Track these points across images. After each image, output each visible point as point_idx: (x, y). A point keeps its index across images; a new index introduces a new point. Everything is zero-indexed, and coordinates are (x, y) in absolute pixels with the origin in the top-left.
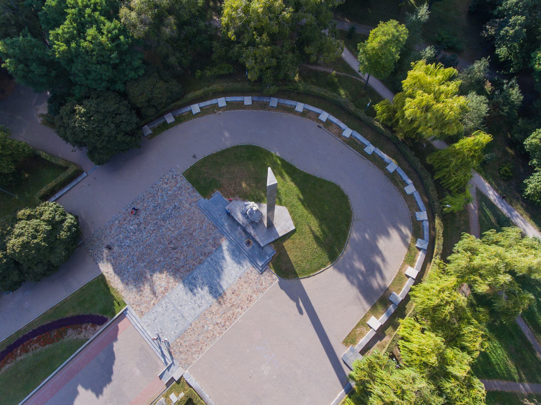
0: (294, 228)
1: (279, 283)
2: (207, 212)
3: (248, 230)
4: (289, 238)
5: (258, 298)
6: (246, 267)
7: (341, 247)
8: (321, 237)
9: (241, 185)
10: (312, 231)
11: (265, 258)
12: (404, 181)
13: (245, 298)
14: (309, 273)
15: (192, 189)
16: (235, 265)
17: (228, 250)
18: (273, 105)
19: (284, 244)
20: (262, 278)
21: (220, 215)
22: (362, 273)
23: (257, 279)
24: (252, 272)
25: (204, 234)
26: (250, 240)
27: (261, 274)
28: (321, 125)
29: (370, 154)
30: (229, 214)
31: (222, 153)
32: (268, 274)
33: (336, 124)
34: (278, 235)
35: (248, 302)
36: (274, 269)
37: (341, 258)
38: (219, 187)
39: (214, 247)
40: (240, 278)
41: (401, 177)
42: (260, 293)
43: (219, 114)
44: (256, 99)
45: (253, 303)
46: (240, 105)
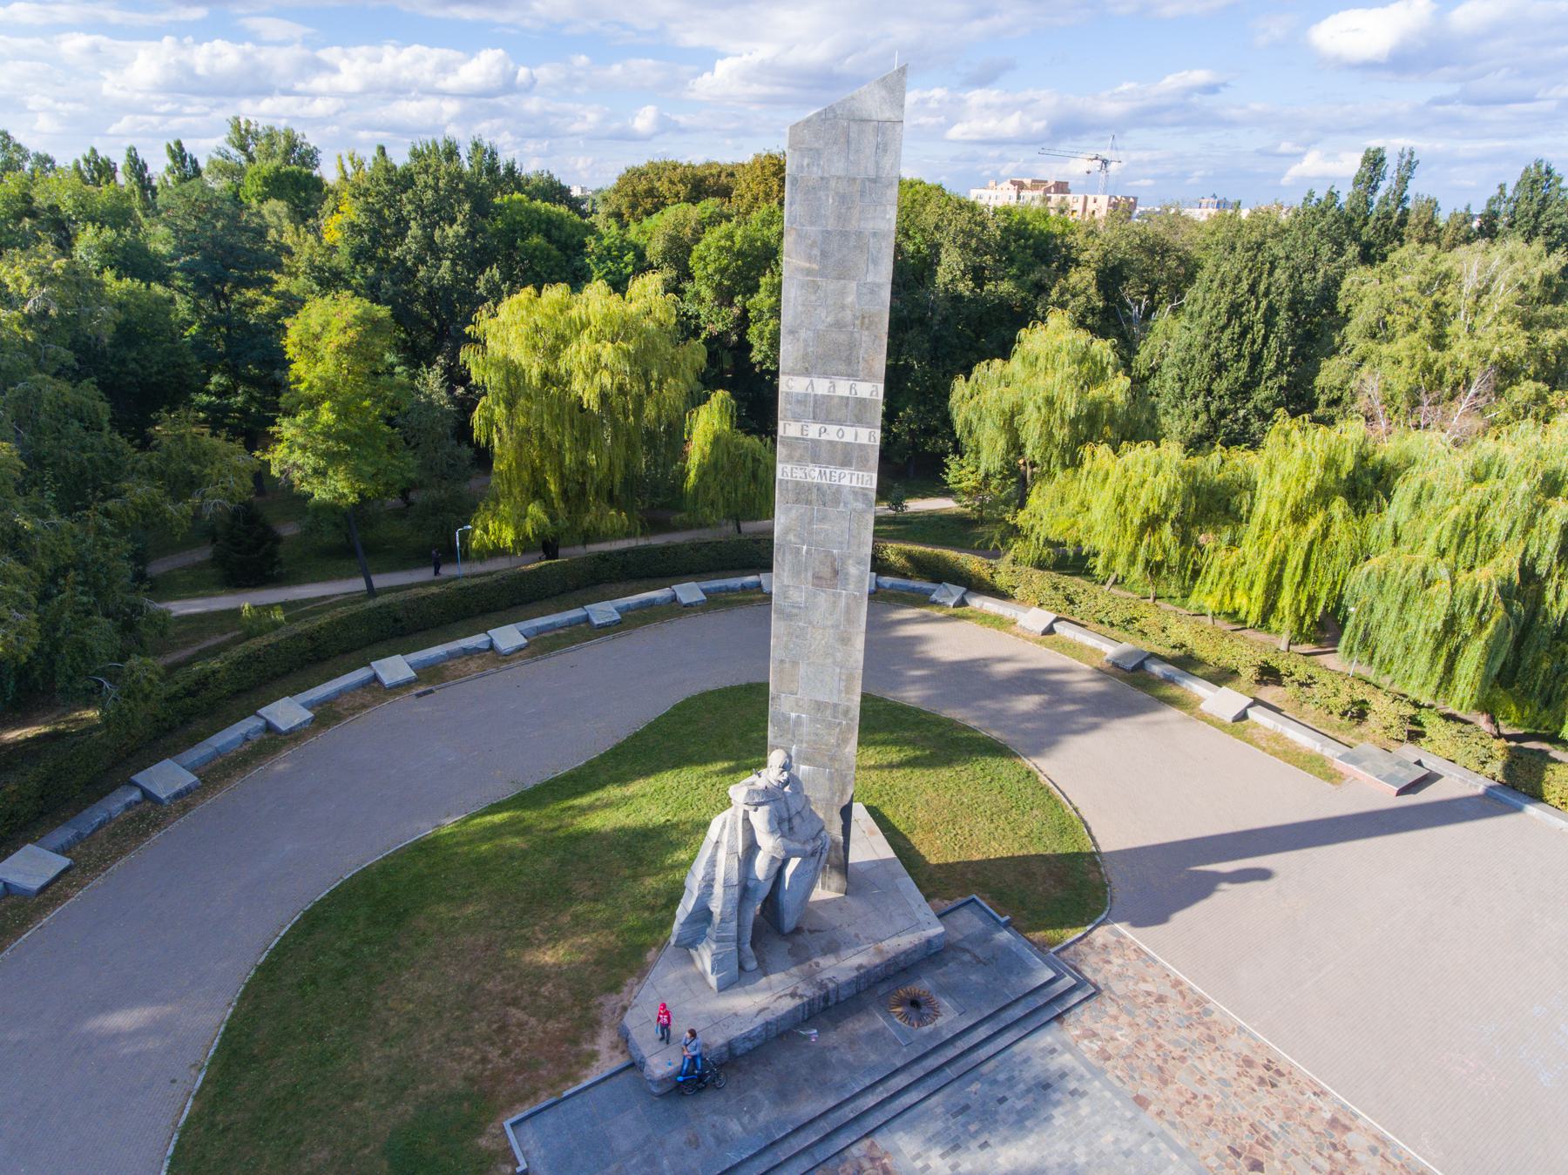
1: (1137, 923)
3: (842, 978)
4: (904, 837)
5: (1241, 1029)
6: (1066, 1060)
7: (952, 724)
8: (909, 753)
9: (542, 974)
10: (880, 767)
11: (1005, 950)
12: (744, 587)
13: (1267, 1098)
14: (1063, 815)
16: (1059, 1117)
17: (956, 1147)
18: (179, 786)
19: (933, 860)
20: (1119, 987)
21: (695, 1143)
22: (1050, 704)
23: (1129, 1013)
24: (1095, 1035)
26: (895, 983)
27: (1098, 992)
28: (422, 689)
29: (618, 617)
30: (701, 1077)
32: (1093, 959)
33: (452, 656)
34: (884, 863)
35: (1283, 1084)
36: (1062, 925)
37: (995, 734)
38: (482, 1102)
40: (1141, 1101)
42: (1208, 1012)
44: (63, 835)
45: (1286, 1058)
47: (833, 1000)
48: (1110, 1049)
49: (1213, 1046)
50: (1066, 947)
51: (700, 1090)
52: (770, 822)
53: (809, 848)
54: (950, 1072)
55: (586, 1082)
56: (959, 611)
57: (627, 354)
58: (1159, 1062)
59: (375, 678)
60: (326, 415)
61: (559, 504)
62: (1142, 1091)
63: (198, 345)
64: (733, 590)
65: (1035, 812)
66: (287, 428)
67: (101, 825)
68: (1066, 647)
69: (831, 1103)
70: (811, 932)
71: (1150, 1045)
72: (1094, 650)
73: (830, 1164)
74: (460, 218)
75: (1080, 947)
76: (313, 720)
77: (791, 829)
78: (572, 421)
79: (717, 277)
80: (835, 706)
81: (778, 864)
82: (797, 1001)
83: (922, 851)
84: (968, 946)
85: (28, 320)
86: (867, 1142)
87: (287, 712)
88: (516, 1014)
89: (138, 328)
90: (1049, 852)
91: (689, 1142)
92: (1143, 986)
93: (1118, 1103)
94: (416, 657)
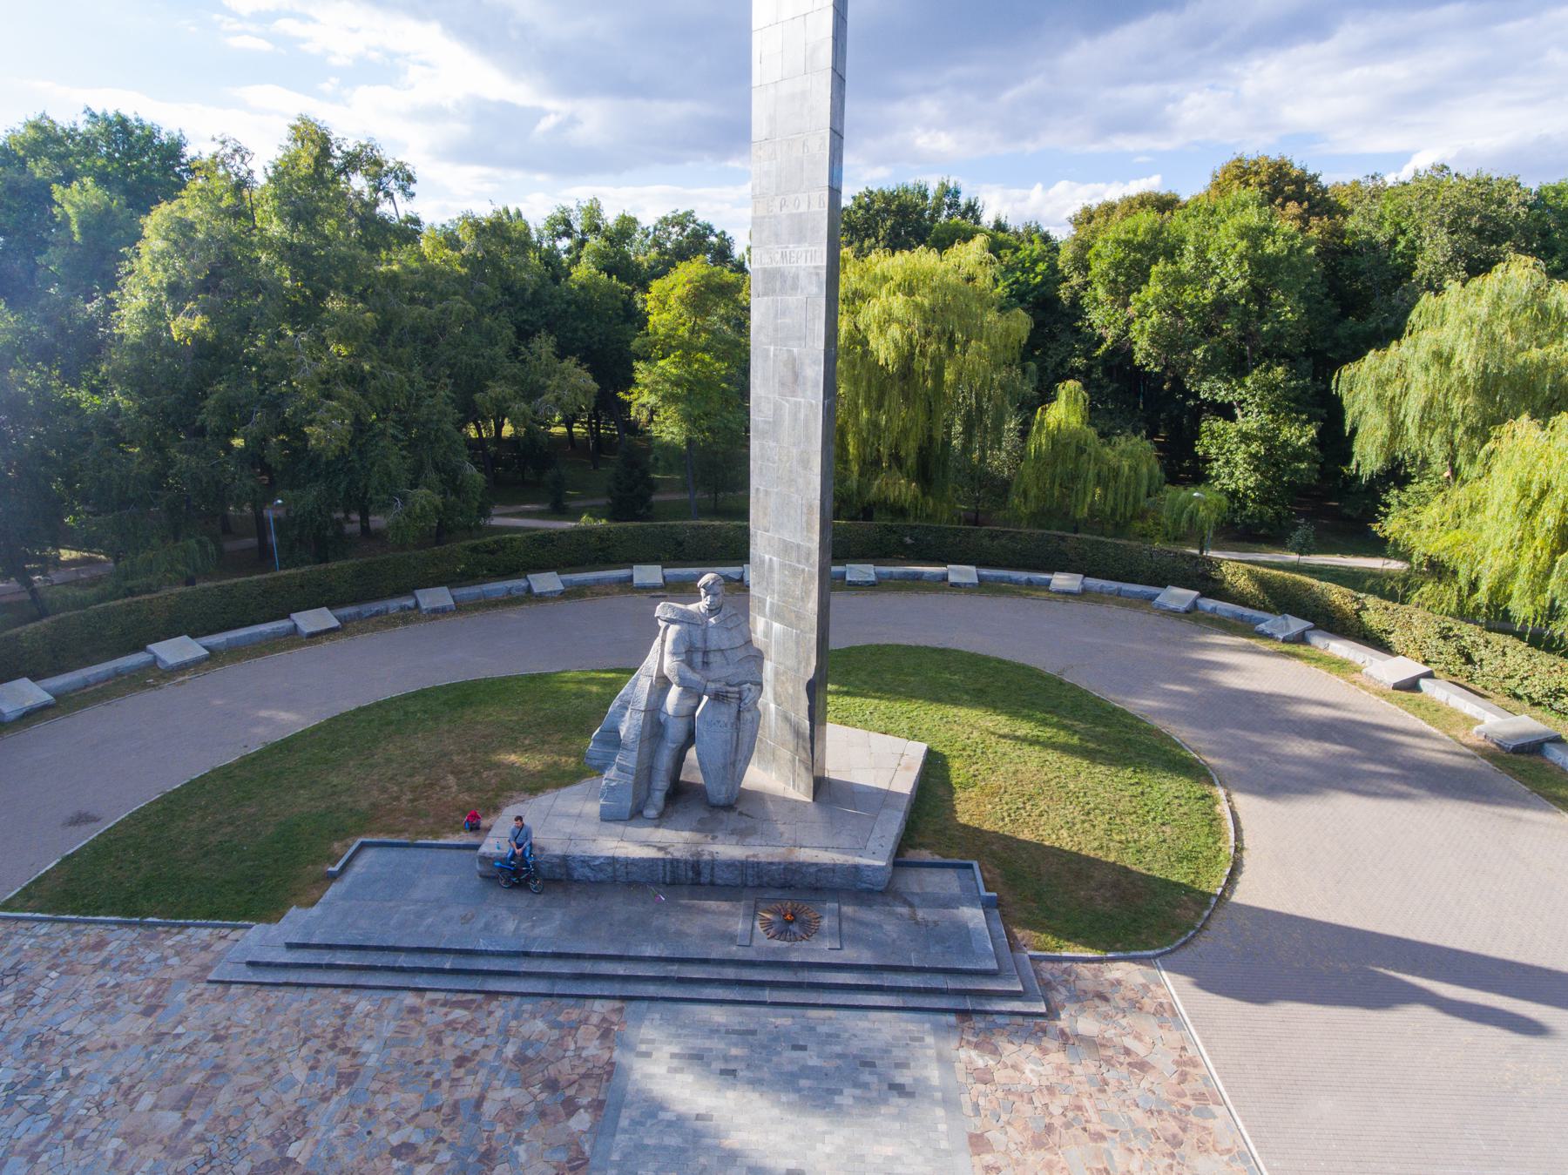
0: (917, 751)
2: (342, 958)
4: (951, 790)
15: (130, 935)
19: (963, 819)
21: (465, 920)
25: (410, 1098)
30: (523, 873)
31: (287, 746)
38: (367, 820)
39: (571, 1108)
41: (1010, 581)
42: (1204, 1113)
43: (183, 683)
46: (294, 638)
47: (705, 878)
48: (1001, 1075)
49: (1168, 1148)
50: (1060, 960)
51: (514, 886)
52: (676, 642)
53: (712, 686)
54: (767, 995)
55: (441, 841)
56: (1286, 647)
57: (918, 307)
58: (1058, 1122)
59: (631, 578)
61: (855, 468)
62: (994, 1135)
64: (1017, 582)
65: (1167, 829)
66: (642, 372)
67: (378, 613)
68: (1436, 712)
69: (611, 951)
70: (741, 813)
71: (1066, 1100)
72: (1470, 721)
73: (564, 1001)
74: (882, 232)
75: (1081, 968)
76: (563, 593)
77: (706, 664)
78: (869, 381)
79: (1112, 274)
80: (798, 546)
81: (691, 702)
82: (660, 855)
83: (958, 808)
84: (916, 901)
85: (464, 261)
86: (618, 1004)
87: (546, 582)
88: (451, 779)
90: (1141, 869)
91: (464, 918)
92: (1129, 1042)
93: (942, 1127)
94: (668, 571)
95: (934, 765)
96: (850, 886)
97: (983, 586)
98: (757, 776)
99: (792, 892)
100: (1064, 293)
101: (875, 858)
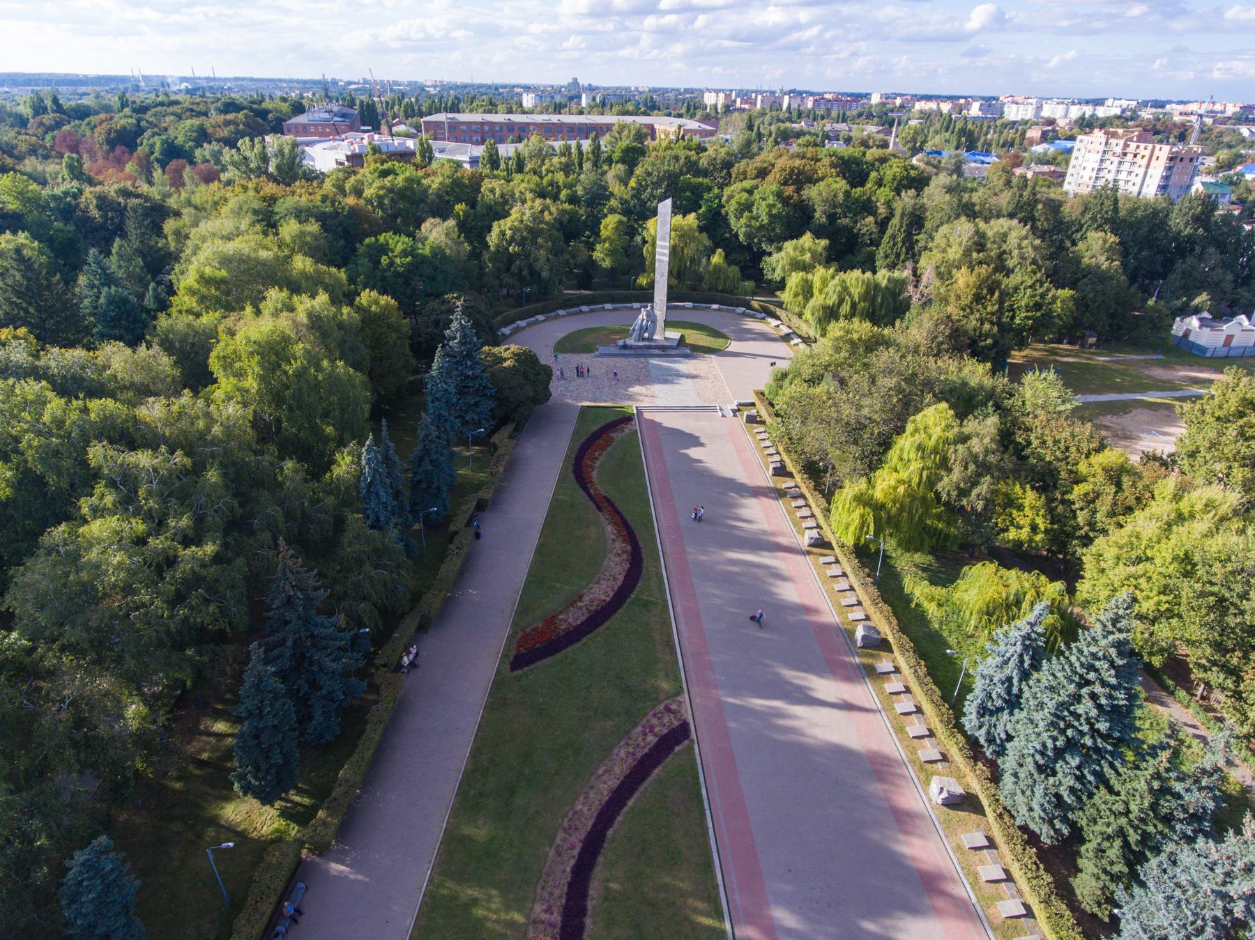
60: (607, 245)
63: (585, 221)
66: (598, 247)
87: (584, 308)
89: (573, 217)
95: (682, 337)
96: (671, 348)
97: (694, 308)
98: (655, 337)
99: (663, 348)
100: (723, 211)
101: (675, 344)
